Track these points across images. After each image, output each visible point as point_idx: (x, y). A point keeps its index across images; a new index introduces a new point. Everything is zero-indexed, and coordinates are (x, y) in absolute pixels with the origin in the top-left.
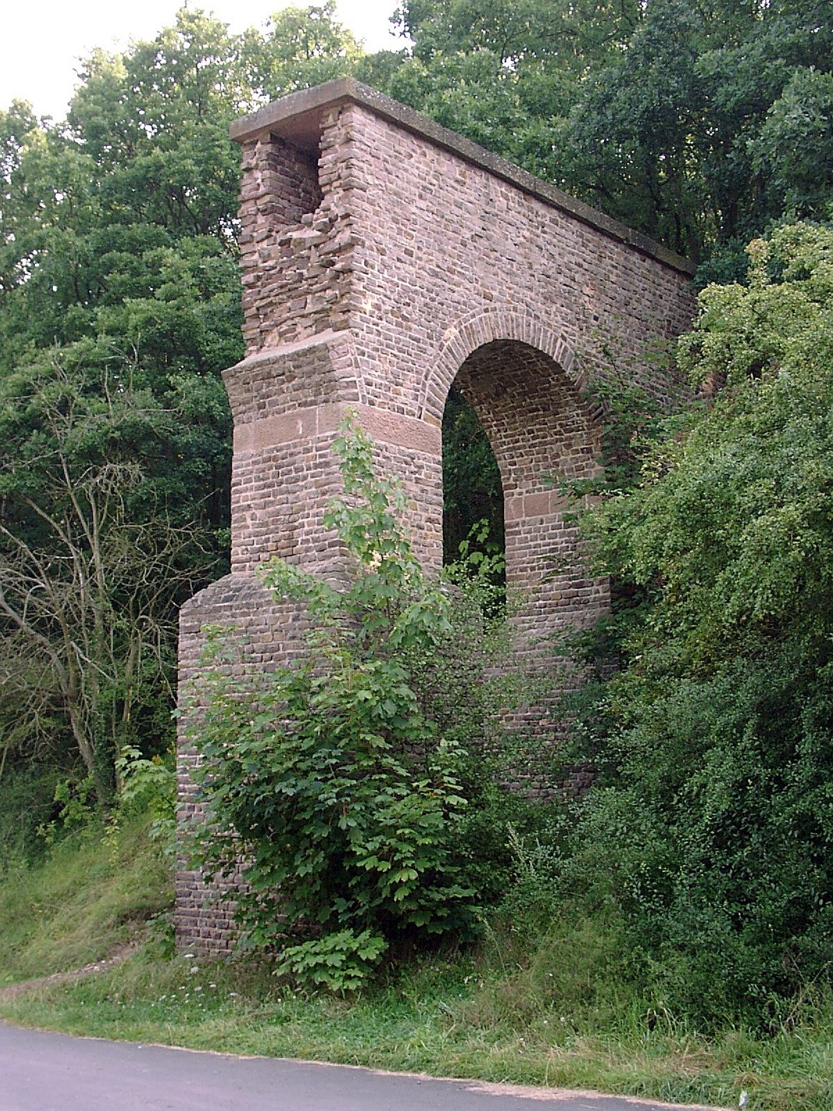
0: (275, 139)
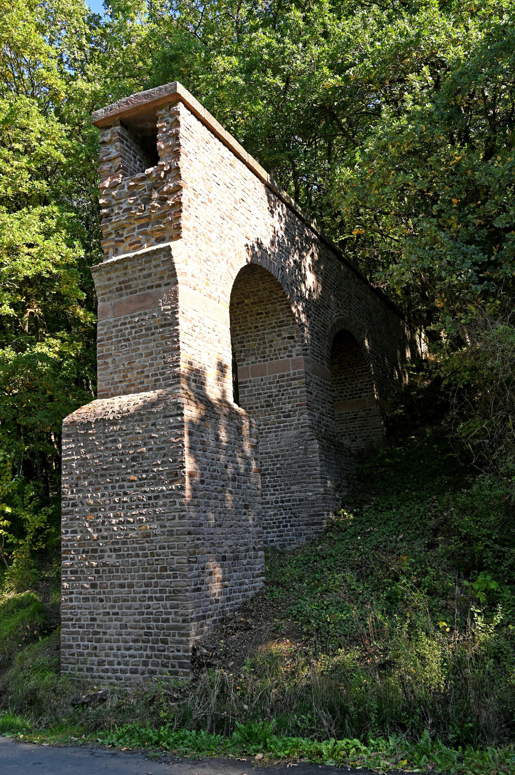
0: (124, 124)
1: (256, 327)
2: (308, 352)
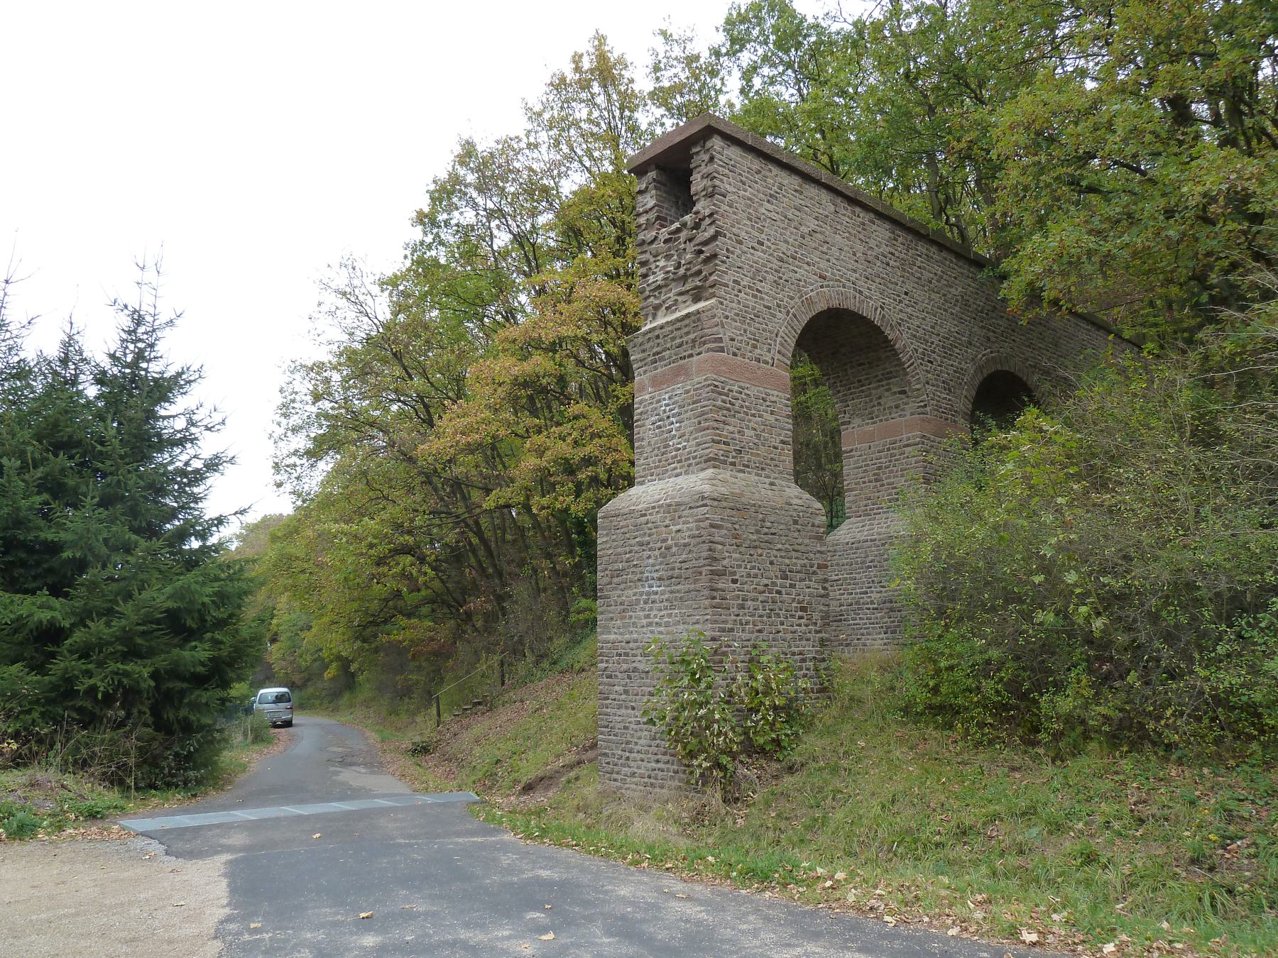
0: (658, 167)
1: (859, 381)
2: (928, 409)
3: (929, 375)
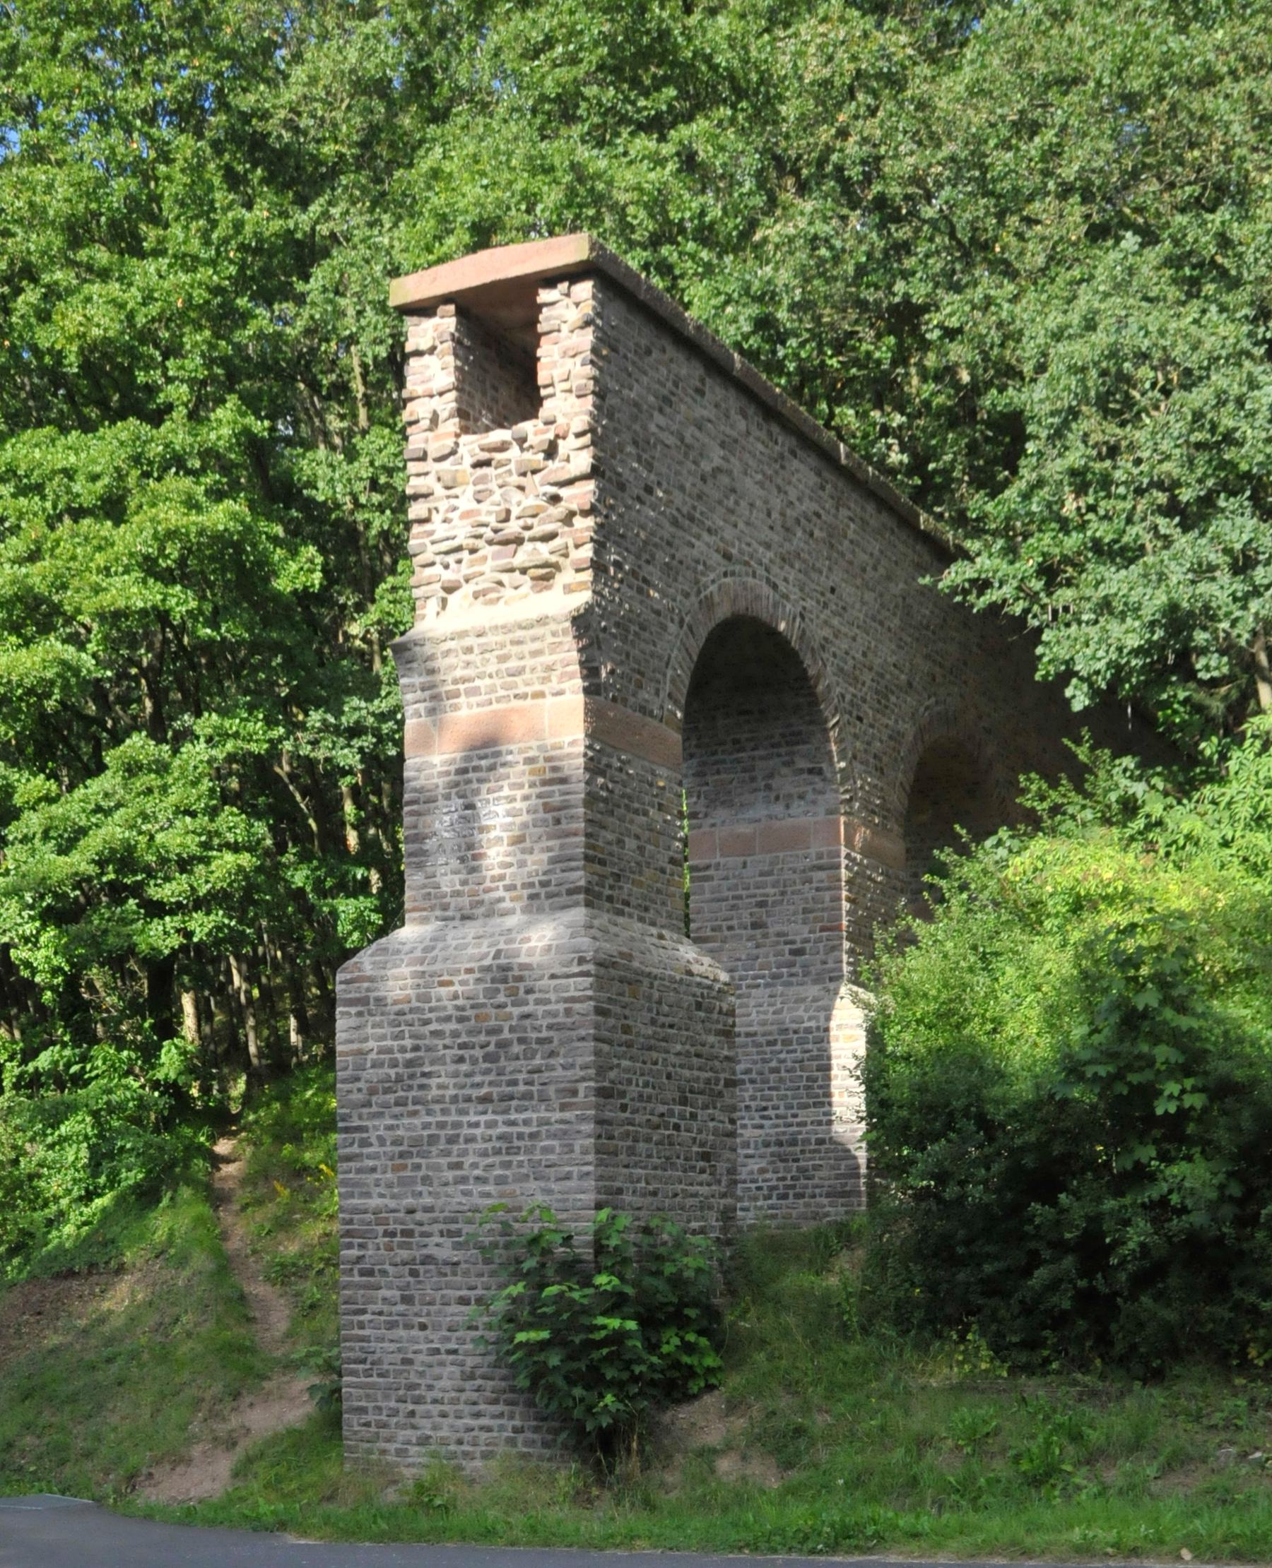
1: (736, 742)
3: (858, 744)
